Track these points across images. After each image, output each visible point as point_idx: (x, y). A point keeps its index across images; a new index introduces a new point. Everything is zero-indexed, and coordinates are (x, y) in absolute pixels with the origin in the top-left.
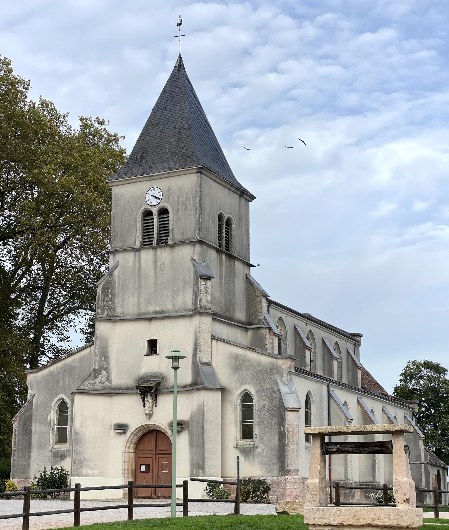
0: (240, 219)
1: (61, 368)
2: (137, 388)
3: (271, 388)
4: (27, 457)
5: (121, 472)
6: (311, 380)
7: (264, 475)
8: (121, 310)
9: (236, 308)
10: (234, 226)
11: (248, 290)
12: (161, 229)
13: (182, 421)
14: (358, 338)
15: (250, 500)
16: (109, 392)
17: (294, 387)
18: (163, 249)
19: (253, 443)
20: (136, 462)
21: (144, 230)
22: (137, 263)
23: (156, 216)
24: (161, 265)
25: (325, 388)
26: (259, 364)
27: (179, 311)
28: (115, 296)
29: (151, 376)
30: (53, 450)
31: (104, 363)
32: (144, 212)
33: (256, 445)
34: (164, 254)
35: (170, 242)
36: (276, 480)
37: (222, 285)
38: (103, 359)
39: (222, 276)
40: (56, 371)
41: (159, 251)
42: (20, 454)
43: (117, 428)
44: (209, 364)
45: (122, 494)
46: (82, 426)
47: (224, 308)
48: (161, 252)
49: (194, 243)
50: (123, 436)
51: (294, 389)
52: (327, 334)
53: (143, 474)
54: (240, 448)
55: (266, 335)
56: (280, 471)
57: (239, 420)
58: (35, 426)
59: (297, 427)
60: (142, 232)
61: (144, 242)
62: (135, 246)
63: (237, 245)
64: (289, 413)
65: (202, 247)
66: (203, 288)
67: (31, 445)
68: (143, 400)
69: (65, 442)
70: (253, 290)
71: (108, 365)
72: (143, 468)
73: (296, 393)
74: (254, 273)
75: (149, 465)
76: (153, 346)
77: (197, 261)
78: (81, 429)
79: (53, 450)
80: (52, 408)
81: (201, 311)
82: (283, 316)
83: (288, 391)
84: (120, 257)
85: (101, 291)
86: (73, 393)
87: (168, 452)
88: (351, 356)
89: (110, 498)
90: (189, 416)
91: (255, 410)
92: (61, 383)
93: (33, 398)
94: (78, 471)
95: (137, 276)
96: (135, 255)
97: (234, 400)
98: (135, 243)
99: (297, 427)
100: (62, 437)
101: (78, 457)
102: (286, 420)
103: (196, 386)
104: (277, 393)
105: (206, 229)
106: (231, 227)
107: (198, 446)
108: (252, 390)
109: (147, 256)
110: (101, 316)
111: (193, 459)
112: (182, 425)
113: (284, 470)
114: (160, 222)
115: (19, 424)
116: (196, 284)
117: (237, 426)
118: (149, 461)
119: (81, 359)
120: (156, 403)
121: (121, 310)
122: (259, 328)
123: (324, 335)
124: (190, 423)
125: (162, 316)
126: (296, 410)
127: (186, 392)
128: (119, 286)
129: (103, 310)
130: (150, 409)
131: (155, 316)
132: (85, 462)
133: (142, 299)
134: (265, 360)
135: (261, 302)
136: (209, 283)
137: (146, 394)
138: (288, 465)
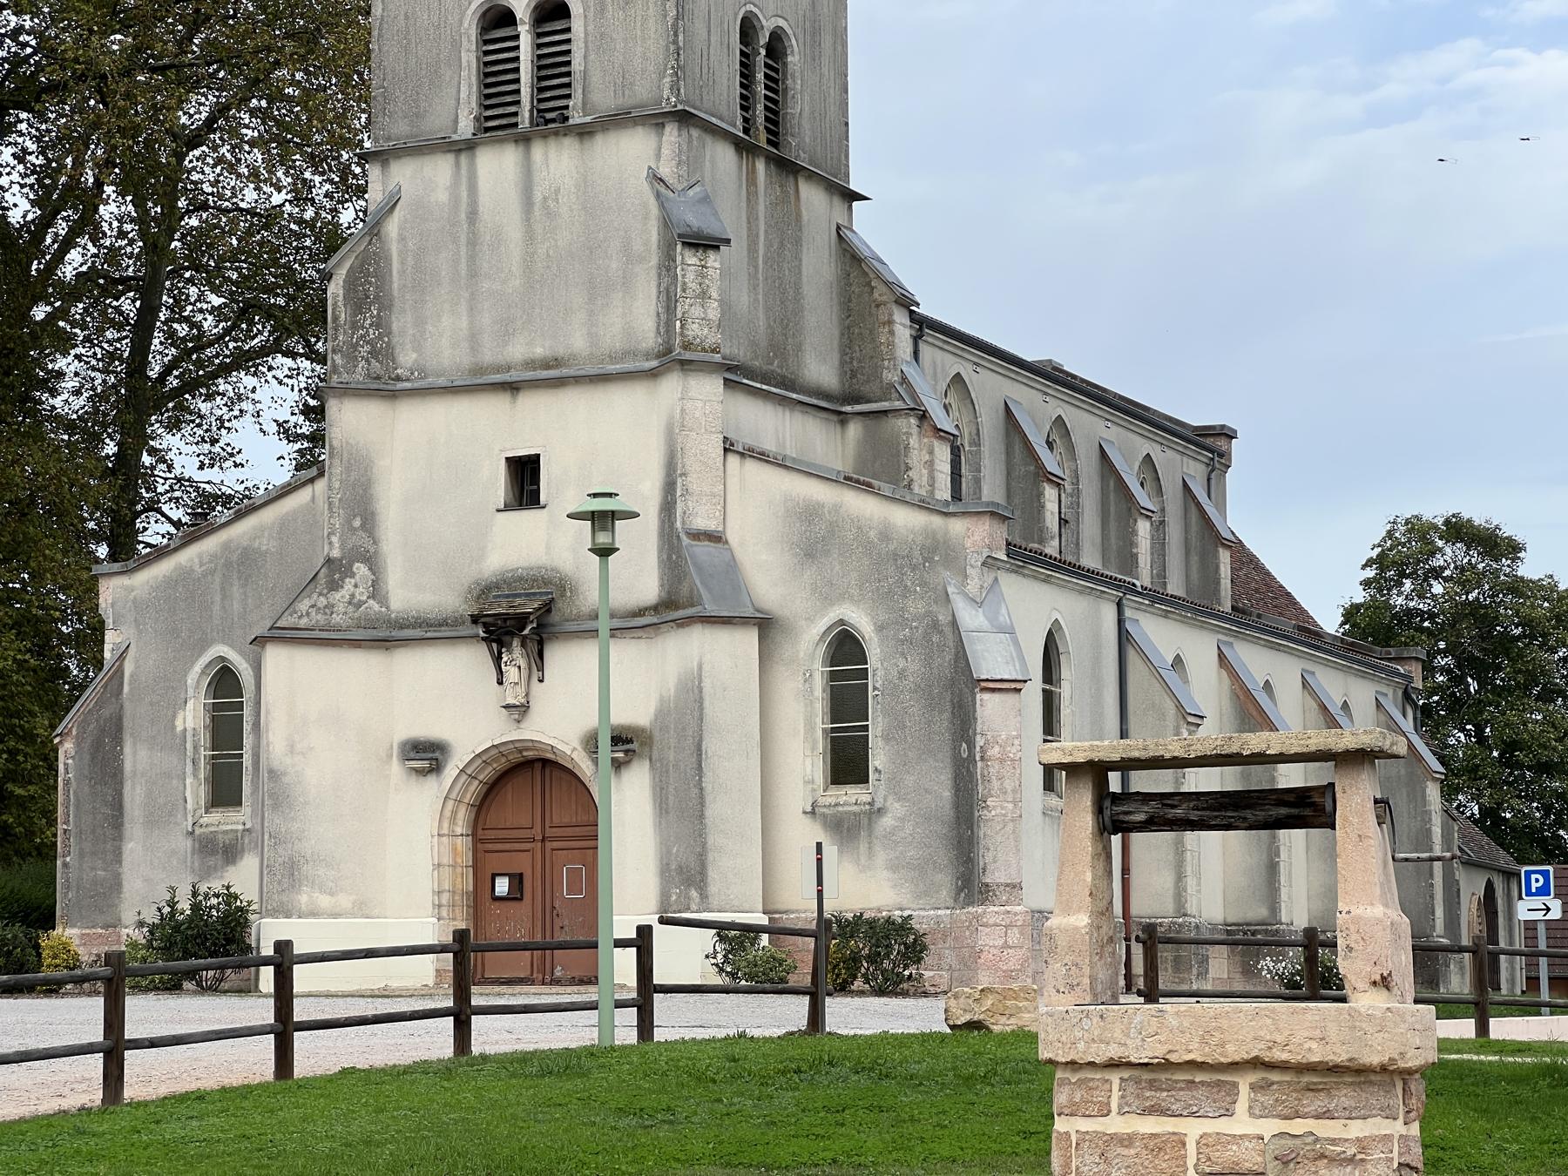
0: (816, 32)
1: (214, 557)
2: (475, 620)
3: (928, 613)
4: (110, 857)
5: (428, 899)
6: (1062, 586)
7: (905, 904)
8: (414, 356)
9: (807, 347)
10: (794, 60)
11: (845, 281)
12: (544, 73)
13: (629, 728)
14: (1221, 443)
15: (858, 984)
17: (1003, 611)
18: (552, 143)
19: (866, 798)
20: (476, 867)
21: (487, 75)
22: (464, 194)
23: (527, 27)
24: (545, 198)
25: (1109, 613)
26: (885, 535)
27: (613, 359)
28: (390, 307)
29: (521, 579)
30: (198, 831)
31: (361, 539)
32: (484, 14)
33: (878, 805)
34: (557, 161)
35: (576, 118)
36: (947, 920)
37: (756, 267)
38: (357, 523)
39: (757, 236)
40: (197, 568)
41: (538, 150)
42: (87, 846)
43: (412, 755)
44: (715, 538)
45: (432, 973)
46: (291, 749)
47: (764, 344)
48: (546, 154)
49: (657, 120)
50: (431, 782)
51: (1003, 618)
52: (1114, 428)
53: (503, 904)
54: (824, 816)
55: (909, 434)
56: (959, 890)
57: (821, 723)
58: (135, 753)
59: (1016, 742)
60: (480, 82)
61: (488, 118)
62: (455, 132)
63: (806, 125)
64: (986, 696)
65: (685, 133)
66: (690, 276)
67: (122, 814)
68: (497, 660)
69: (237, 802)
70: (862, 282)
71: (375, 543)
72: (502, 886)
73: (1010, 631)
74: (866, 225)
76: (524, 478)
77: (670, 181)
78: (288, 761)
79: (198, 831)
80: (190, 692)
81: (688, 356)
82: (966, 371)
83: (986, 624)
84: (405, 175)
85: (341, 292)
86: (260, 641)
87: (585, 834)
88: (1198, 505)
89: (394, 984)
90: (652, 711)
91: (875, 688)
92: (216, 608)
93: (122, 657)
95: (463, 239)
96: (457, 165)
98: (456, 121)
99: (1016, 742)
100: (225, 788)
101: (280, 851)
102: (979, 721)
103: (674, 609)
104: (948, 630)
105: (697, 70)
106: (785, 64)
107: (684, 809)
108: (863, 622)
109: (497, 166)
110: (345, 377)
111: (669, 852)
112: (630, 741)
113: (971, 885)
114: (539, 46)
115: (78, 744)
116: (668, 264)
117: (815, 742)
118: (522, 863)
119: (283, 524)
120: (541, 669)
121: (414, 356)
122: (885, 412)
123: (1106, 434)
124: (657, 735)
125: (553, 376)
126: (1013, 687)
127: (640, 633)
128: (402, 272)
129: (352, 358)
130: (521, 691)
131: (529, 375)
133: (486, 319)
134: (905, 520)
135: (890, 322)
136: (713, 260)
137: (506, 639)
138: (984, 870)
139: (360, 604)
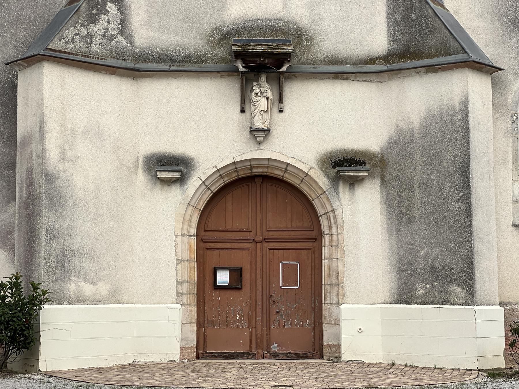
16: (131, 65)
29: (260, 28)
43: (158, 167)
46: (63, 156)
50: (175, 191)
53: (223, 293)
72: (223, 278)
75: (241, 269)
78: (61, 166)
86: (31, 60)
94: (58, 288)
97: (510, 101)
112: (362, 163)
118: (240, 259)
120: (281, 100)
127: (374, 77)
132: (75, 261)
139: (111, 38)
